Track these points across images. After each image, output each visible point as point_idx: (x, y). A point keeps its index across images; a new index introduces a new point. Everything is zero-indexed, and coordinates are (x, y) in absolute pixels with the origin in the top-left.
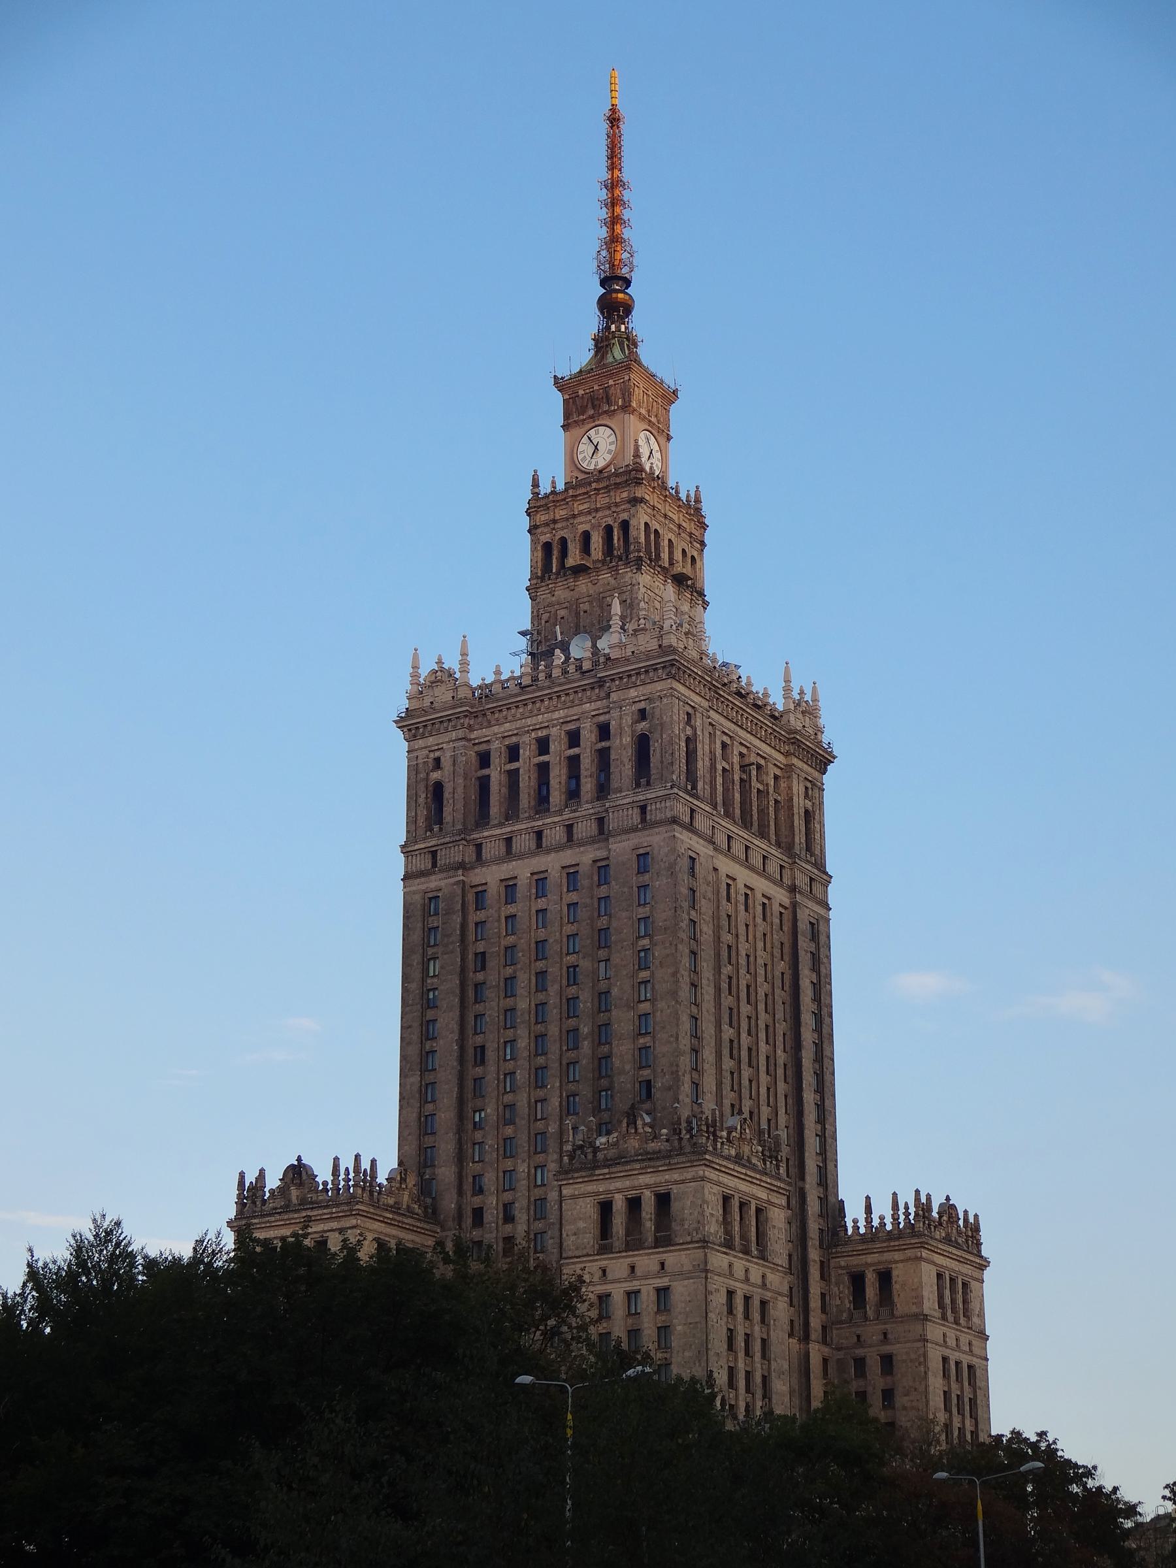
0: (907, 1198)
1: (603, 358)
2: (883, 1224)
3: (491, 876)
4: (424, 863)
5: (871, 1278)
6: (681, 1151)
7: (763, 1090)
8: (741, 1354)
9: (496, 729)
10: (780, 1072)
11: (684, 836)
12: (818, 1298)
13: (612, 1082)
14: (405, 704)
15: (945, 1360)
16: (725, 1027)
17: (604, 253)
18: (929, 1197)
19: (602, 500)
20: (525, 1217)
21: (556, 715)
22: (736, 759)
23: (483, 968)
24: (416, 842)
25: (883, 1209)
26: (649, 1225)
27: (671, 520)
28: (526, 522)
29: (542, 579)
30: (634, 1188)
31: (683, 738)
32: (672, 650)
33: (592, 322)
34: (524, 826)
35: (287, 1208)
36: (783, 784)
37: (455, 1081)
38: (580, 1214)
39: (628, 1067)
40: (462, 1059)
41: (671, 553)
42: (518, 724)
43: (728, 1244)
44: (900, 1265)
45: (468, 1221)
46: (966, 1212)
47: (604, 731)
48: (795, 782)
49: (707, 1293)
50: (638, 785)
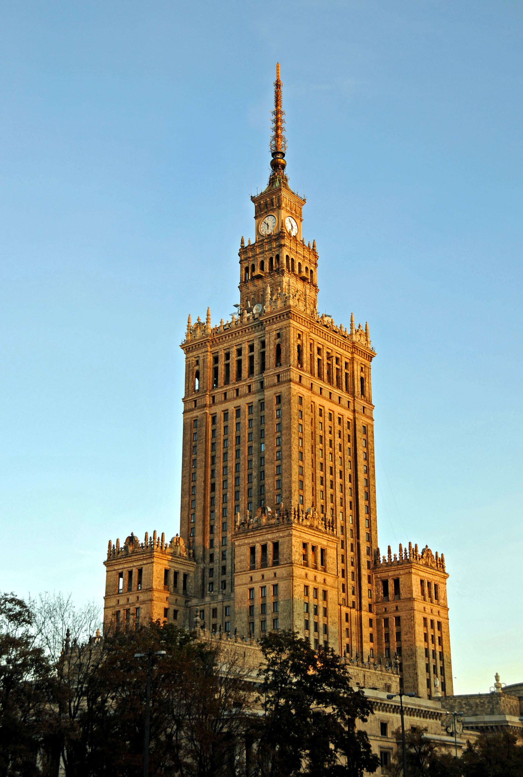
0: (405, 546)
1: (272, 186)
2: (395, 558)
9: (221, 346)
15: (425, 619)
16: (318, 471)
17: (273, 142)
20: (230, 557)
21: (244, 339)
22: (325, 355)
24: (188, 397)
25: (395, 551)
27: (299, 254)
28: (238, 259)
30: (263, 541)
33: (268, 171)
34: (231, 387)
35: (127, 555)
36: (350, 366)
37: (203, 498)
38: (242, 554)
42: (229, 344)
44: (403, 576)
45: (208, 560)
47: (263, 344)
50: (277, 366)
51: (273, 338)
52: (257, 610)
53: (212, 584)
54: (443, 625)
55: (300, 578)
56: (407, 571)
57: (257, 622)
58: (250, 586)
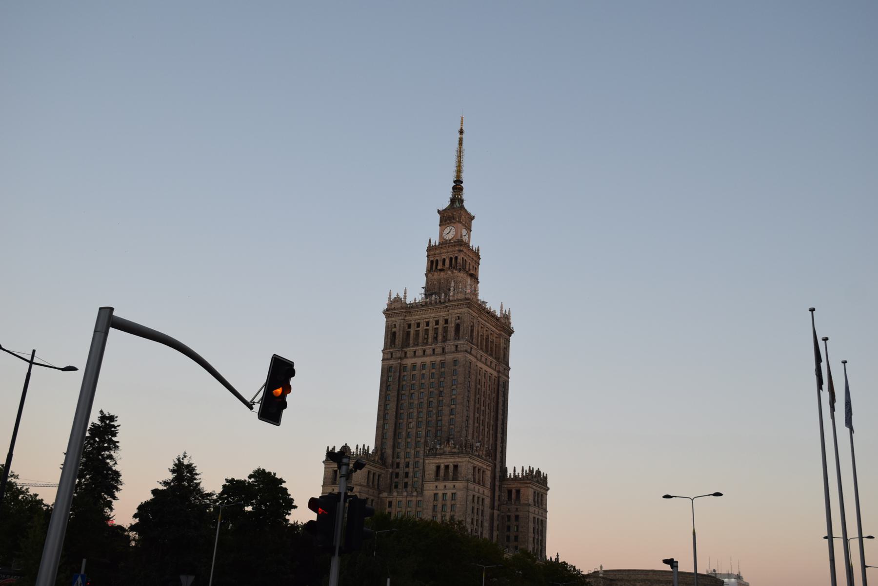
0: (526, 468)
3: (409, 362)
4: (389, 356)
5: (514, 491)
6: (462, 453)
19: (450, 249)
25: (519, 471)
26: (451, 474)
32: (468, 299)
33: (449, 194)
38: (431, 469)
40: (396, 417)
43: (474, 481)
47: (446, 321)
51: (454, 319)
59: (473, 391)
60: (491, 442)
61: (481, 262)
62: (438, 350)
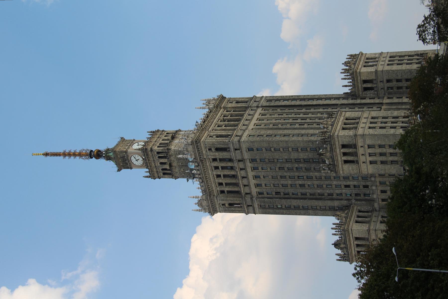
0: (343, 76)
2: (350, 82)
3: (254, 191)
5: (365, 85)
6: (330, 142)
7: (313, 116)
8: (386, 125)
9: (214, 189)
10: (308, 111)
11: (243, 139)
12: (371, 100)
13: (311, 158)
14: (207, 213)
15: (388, 65)
16: (296, 127)
17: (83, 157)
18: (343, 70)
19: (151, 159)
20: (348, 182)
21: (210, 173)
22: (222, 123)
23: (280, 193)
25: (346, 82)
26: (350, 150)
27: (156, 140)
28: (157, 180)
29: (173, 175)
30: (340, 155)
31: (216, 138)
32: (192, 142)
33: (102, 161)
35: (346, 248)
36: (229, 109)
37: (311, 201)
39: (307, 154)
40: (305, 199)
41: (166, 140)
42: (213, 183)
43: (356, 128)
46: (347, 59)
47: (214, 160)
48: (228, 106)
49: (369, 135)
50: (229, 151)
52: (383, 158)
53: (365, 195)
54: (392, 55)
55: (364, 131)
56: (358, 75)
57: (391, 158)
58: (368, 163)
59: (275, 132)
60: (321, 110)
61: (161, 129)
62: (241, 165)
